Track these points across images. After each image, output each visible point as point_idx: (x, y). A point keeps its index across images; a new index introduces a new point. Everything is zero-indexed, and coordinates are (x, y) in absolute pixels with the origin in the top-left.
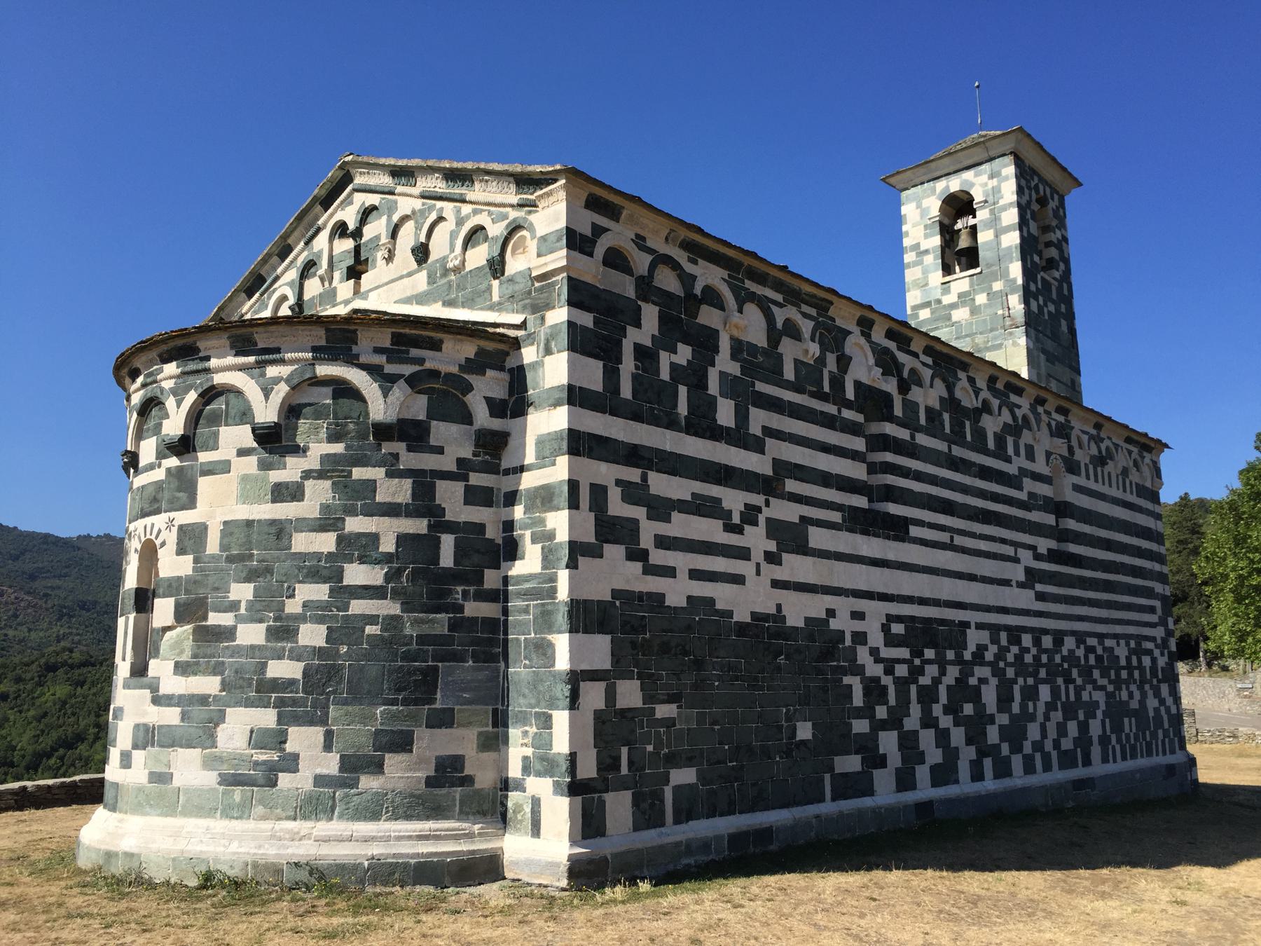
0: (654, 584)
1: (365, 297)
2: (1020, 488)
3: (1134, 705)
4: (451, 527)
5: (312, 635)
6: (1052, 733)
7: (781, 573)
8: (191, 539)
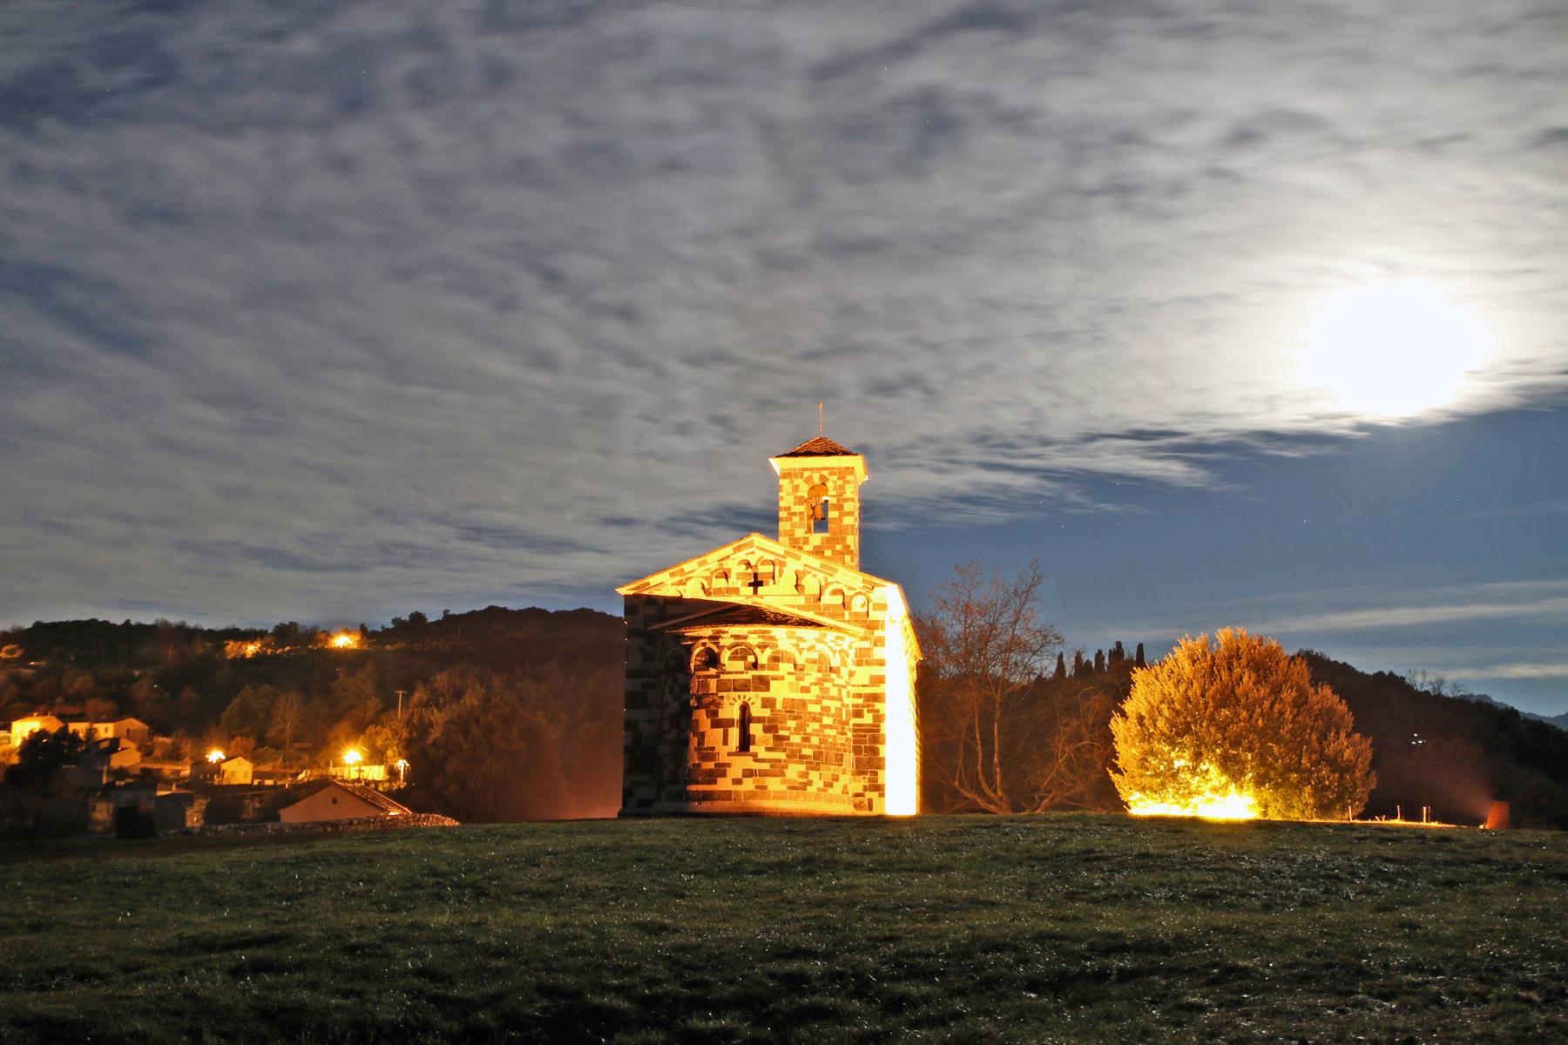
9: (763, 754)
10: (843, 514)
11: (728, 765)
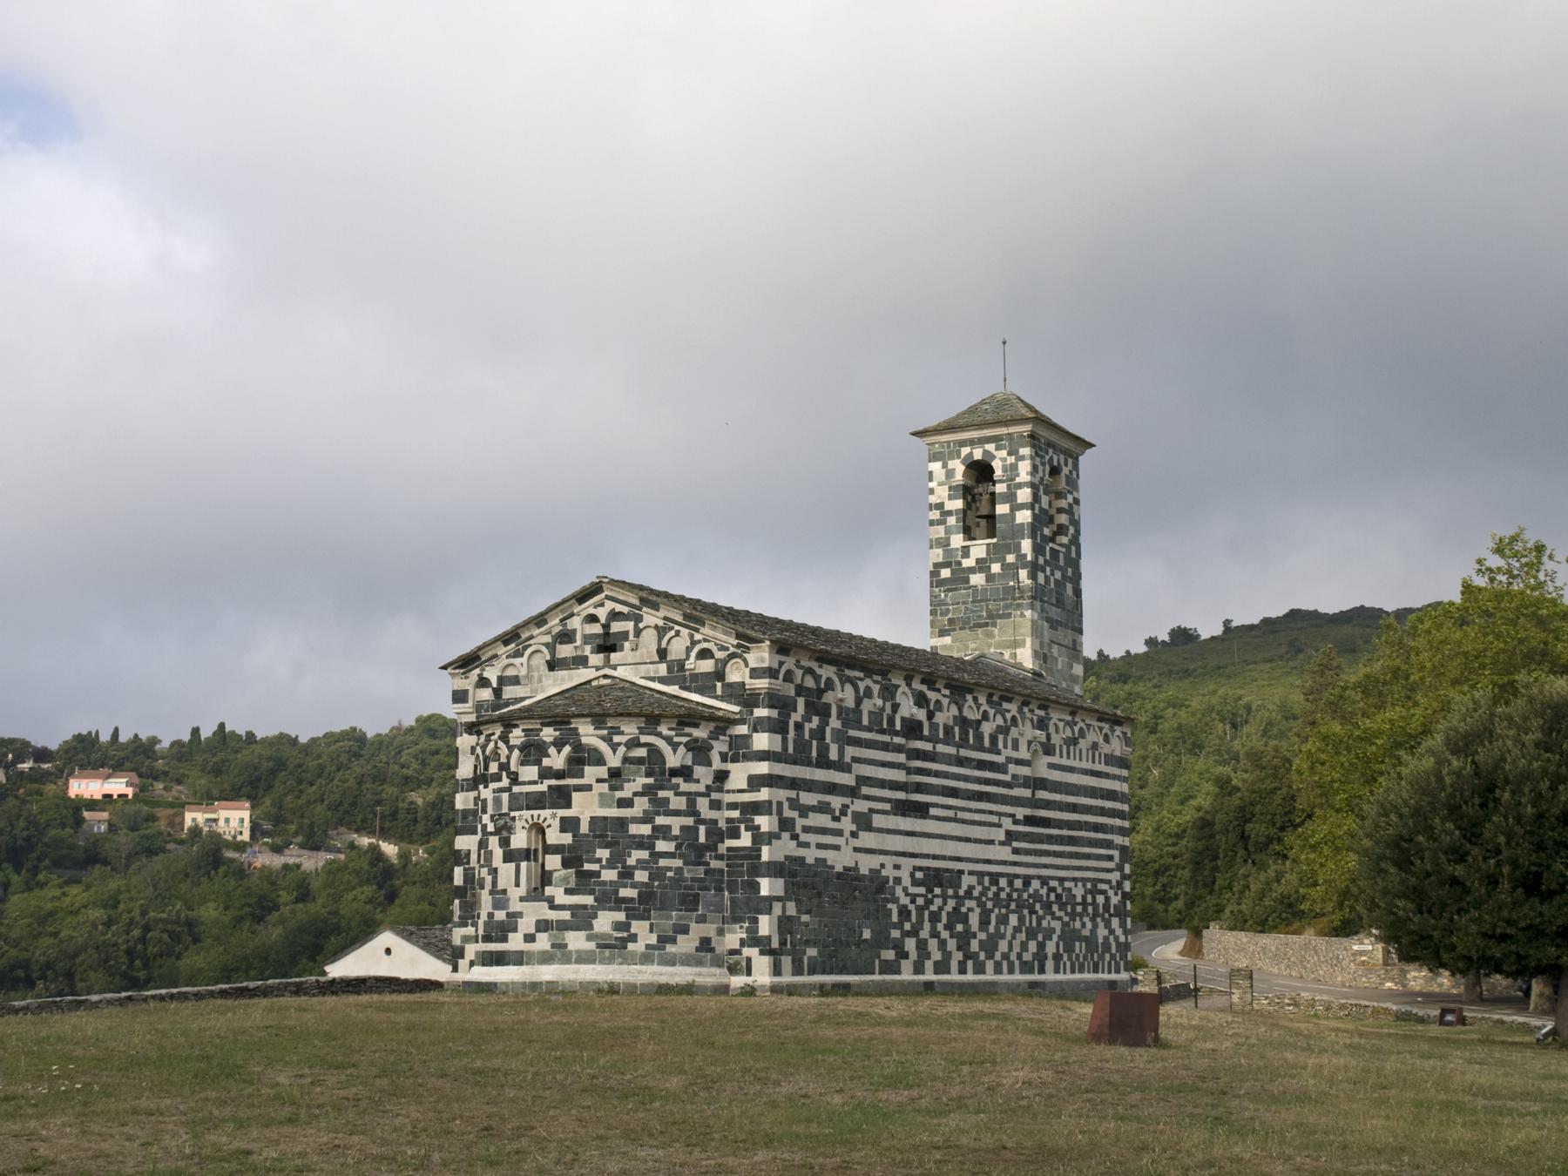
0: (801, 852)
1: (614, 668)
2: (1005, 772)
3: (1086, 932)
4: (703, 822)
5: (641, 876)
6: (1017, 949)
7: (858, 843)
8: (569, 825)
9: (561, 898)
10: (1016, 507)
11: (520, 915)
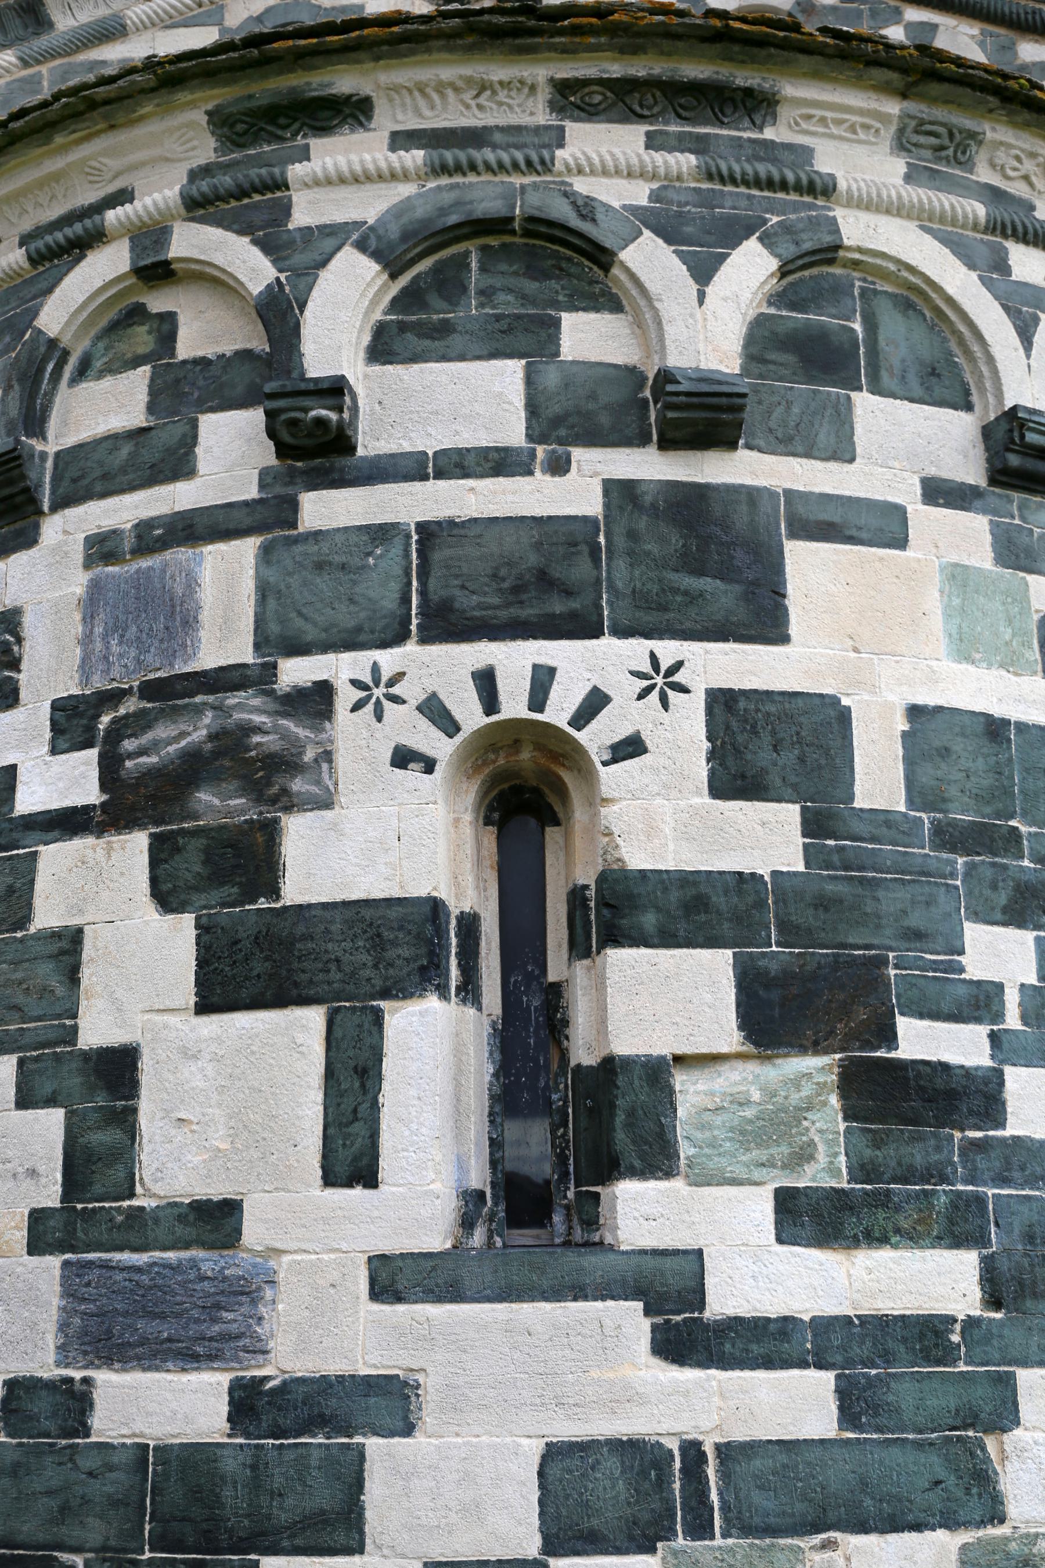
8: (766, 746)
9: (757, 1272)
11: (389, 1402)
